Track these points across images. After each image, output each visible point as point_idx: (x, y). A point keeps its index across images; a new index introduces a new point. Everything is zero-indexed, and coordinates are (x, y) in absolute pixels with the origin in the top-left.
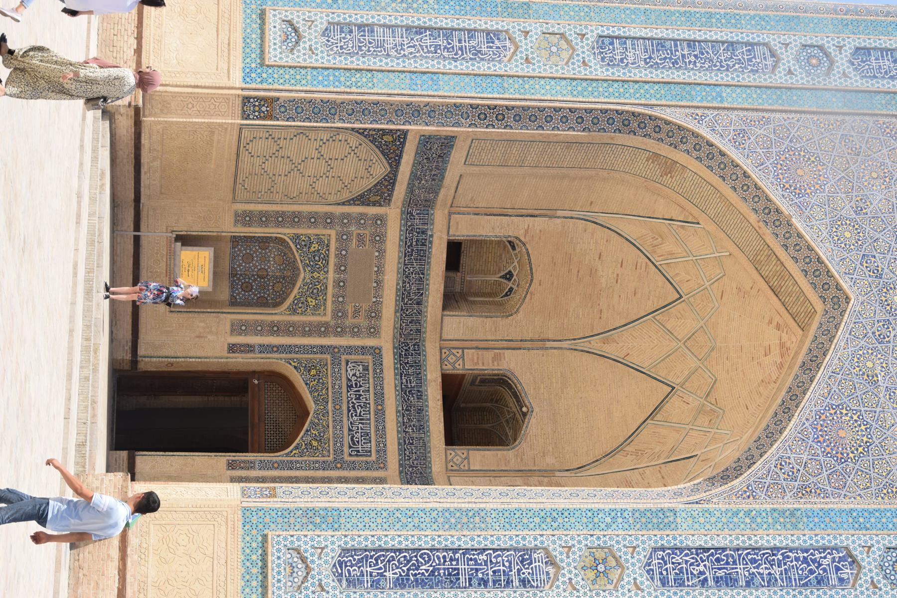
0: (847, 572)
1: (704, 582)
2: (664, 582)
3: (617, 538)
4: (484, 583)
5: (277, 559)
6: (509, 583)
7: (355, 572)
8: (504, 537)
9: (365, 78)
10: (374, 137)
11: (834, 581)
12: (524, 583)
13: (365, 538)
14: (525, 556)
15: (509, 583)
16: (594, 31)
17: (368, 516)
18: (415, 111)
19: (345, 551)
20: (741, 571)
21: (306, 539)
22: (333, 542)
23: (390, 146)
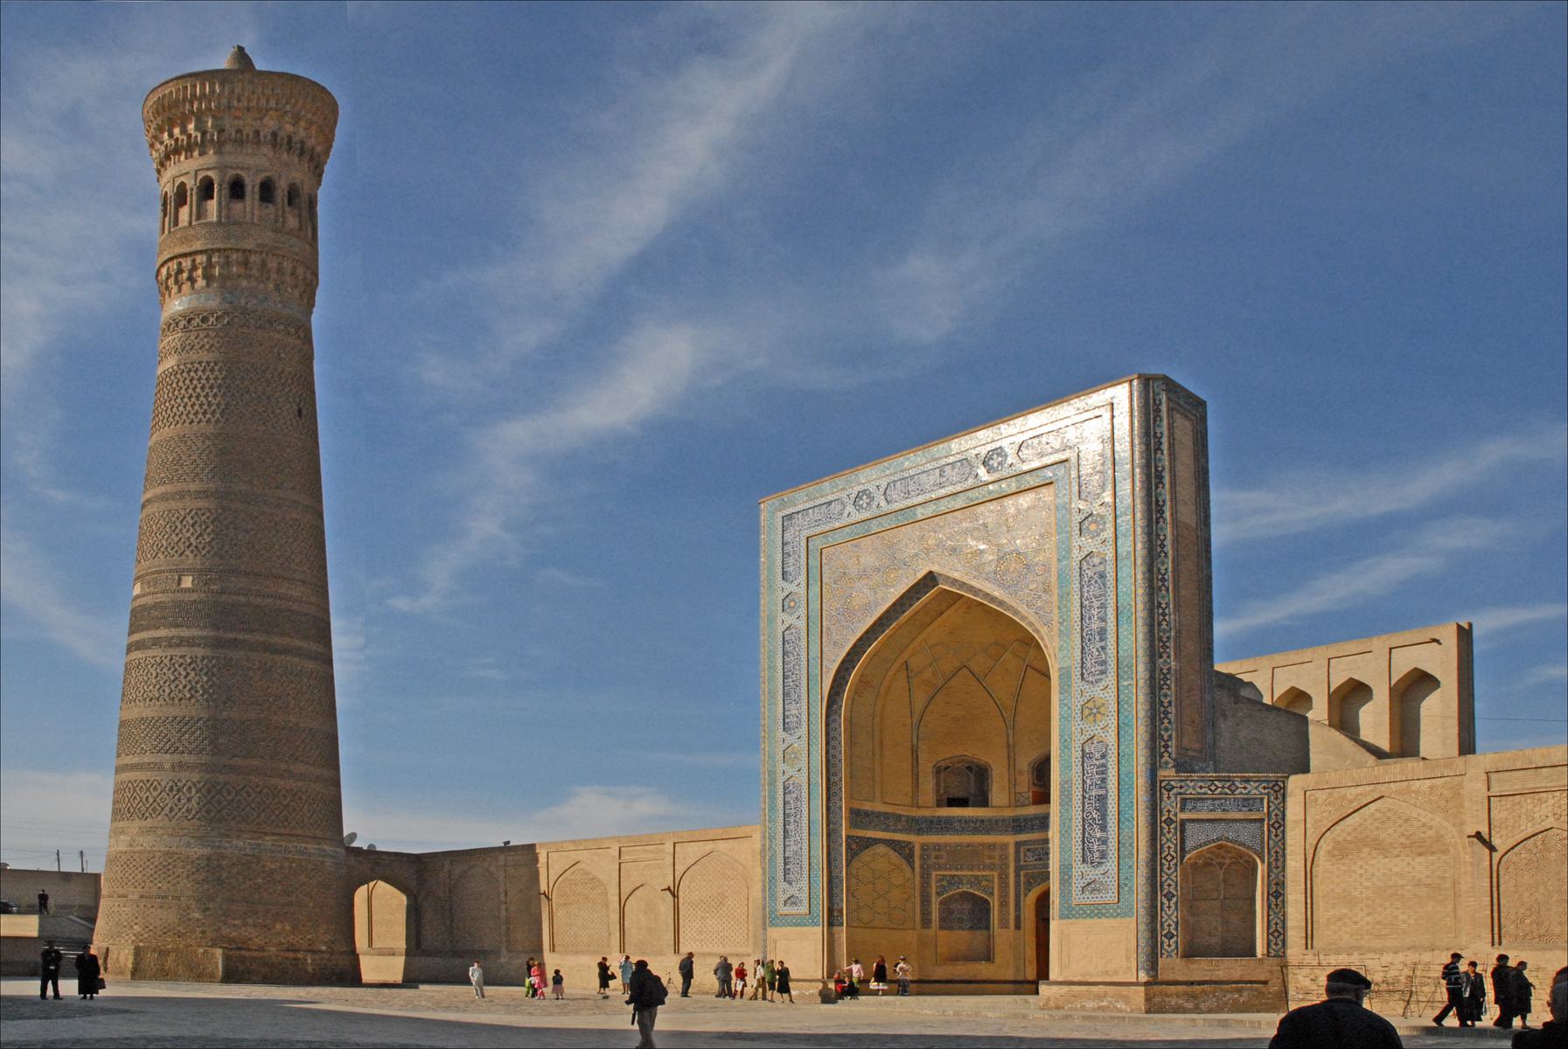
0: (1096, 560)
1: (1103, 648)
2: (1102, 672)
3: (1077, 702)
4: (1104, 780)
5: (1089, 898)
6: (1104, 765)
7: (1097, 855)
8: (1076, 769)
9: (814, 861)
10: (852, 855)
11: (1101, 568)
12: (1103, 756)
13: (1077, 849)
14: (1085, 756)
15: (1104, 765)
16: (781, 734)
17: (1065, 849)
18: (831, 834)
19: (1084, 861)
20: (1096, 625)
21: (1077, 883)
22: (1078, 868)
23: (858, 846)
